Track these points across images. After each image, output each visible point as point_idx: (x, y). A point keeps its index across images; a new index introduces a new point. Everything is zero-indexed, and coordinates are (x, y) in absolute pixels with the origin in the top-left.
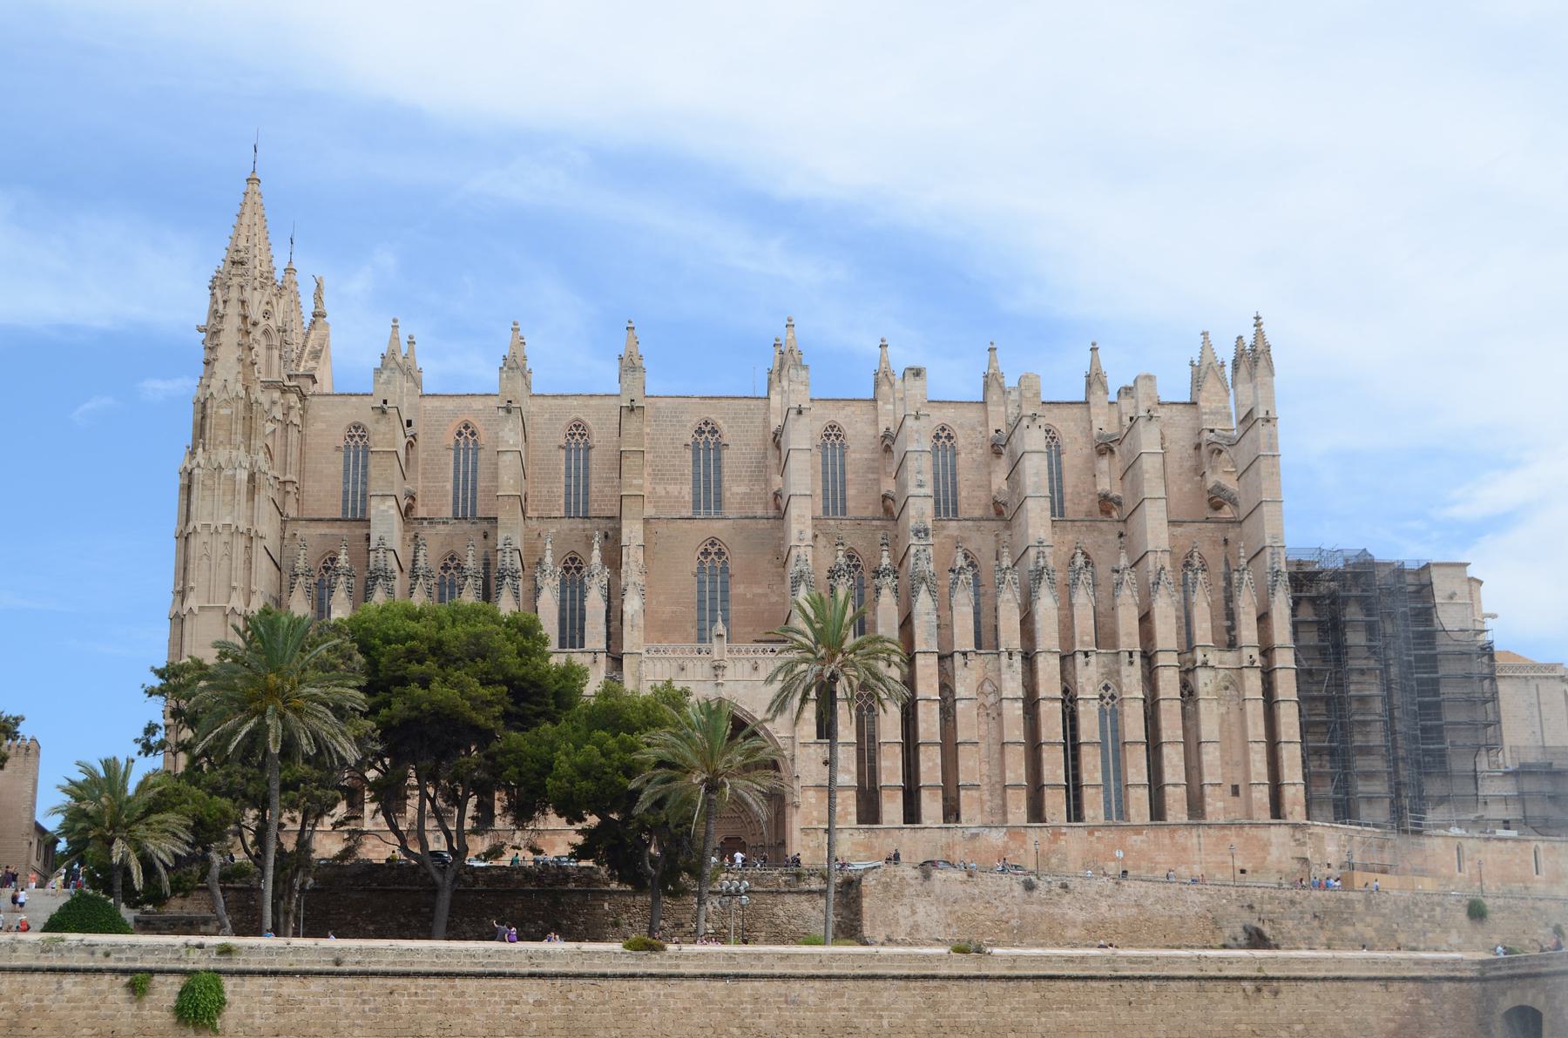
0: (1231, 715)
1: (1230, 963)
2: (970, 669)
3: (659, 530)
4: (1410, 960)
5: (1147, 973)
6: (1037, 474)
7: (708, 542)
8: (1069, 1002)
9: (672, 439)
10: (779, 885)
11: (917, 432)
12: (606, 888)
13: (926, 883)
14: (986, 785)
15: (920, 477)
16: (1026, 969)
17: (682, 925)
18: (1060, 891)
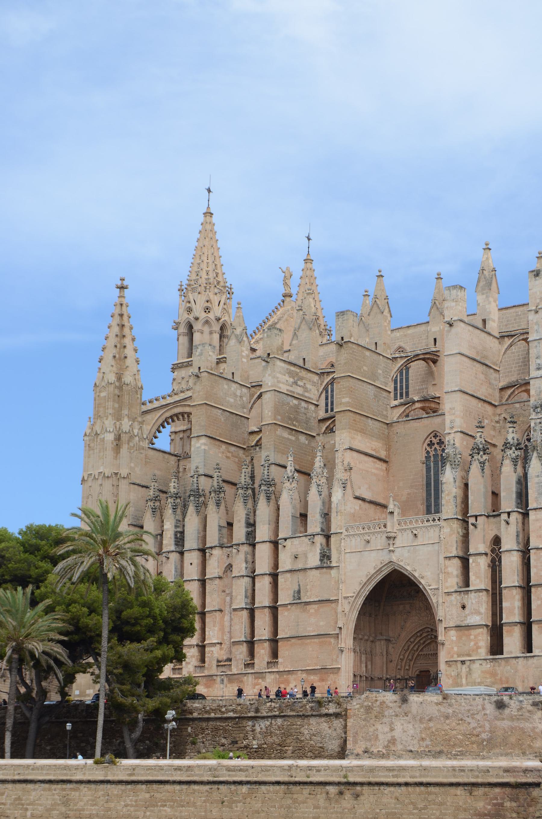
1: (318, 771)
3: (398, 431)
4: (500, 768)
5: (244, 779)
7: (432, 435)
8: (173, 801)
10: (306, 710)
12: (191, 716)
13: (404, 706)
16: (142, 775)
17: (236, 742)
18: (530, 708)
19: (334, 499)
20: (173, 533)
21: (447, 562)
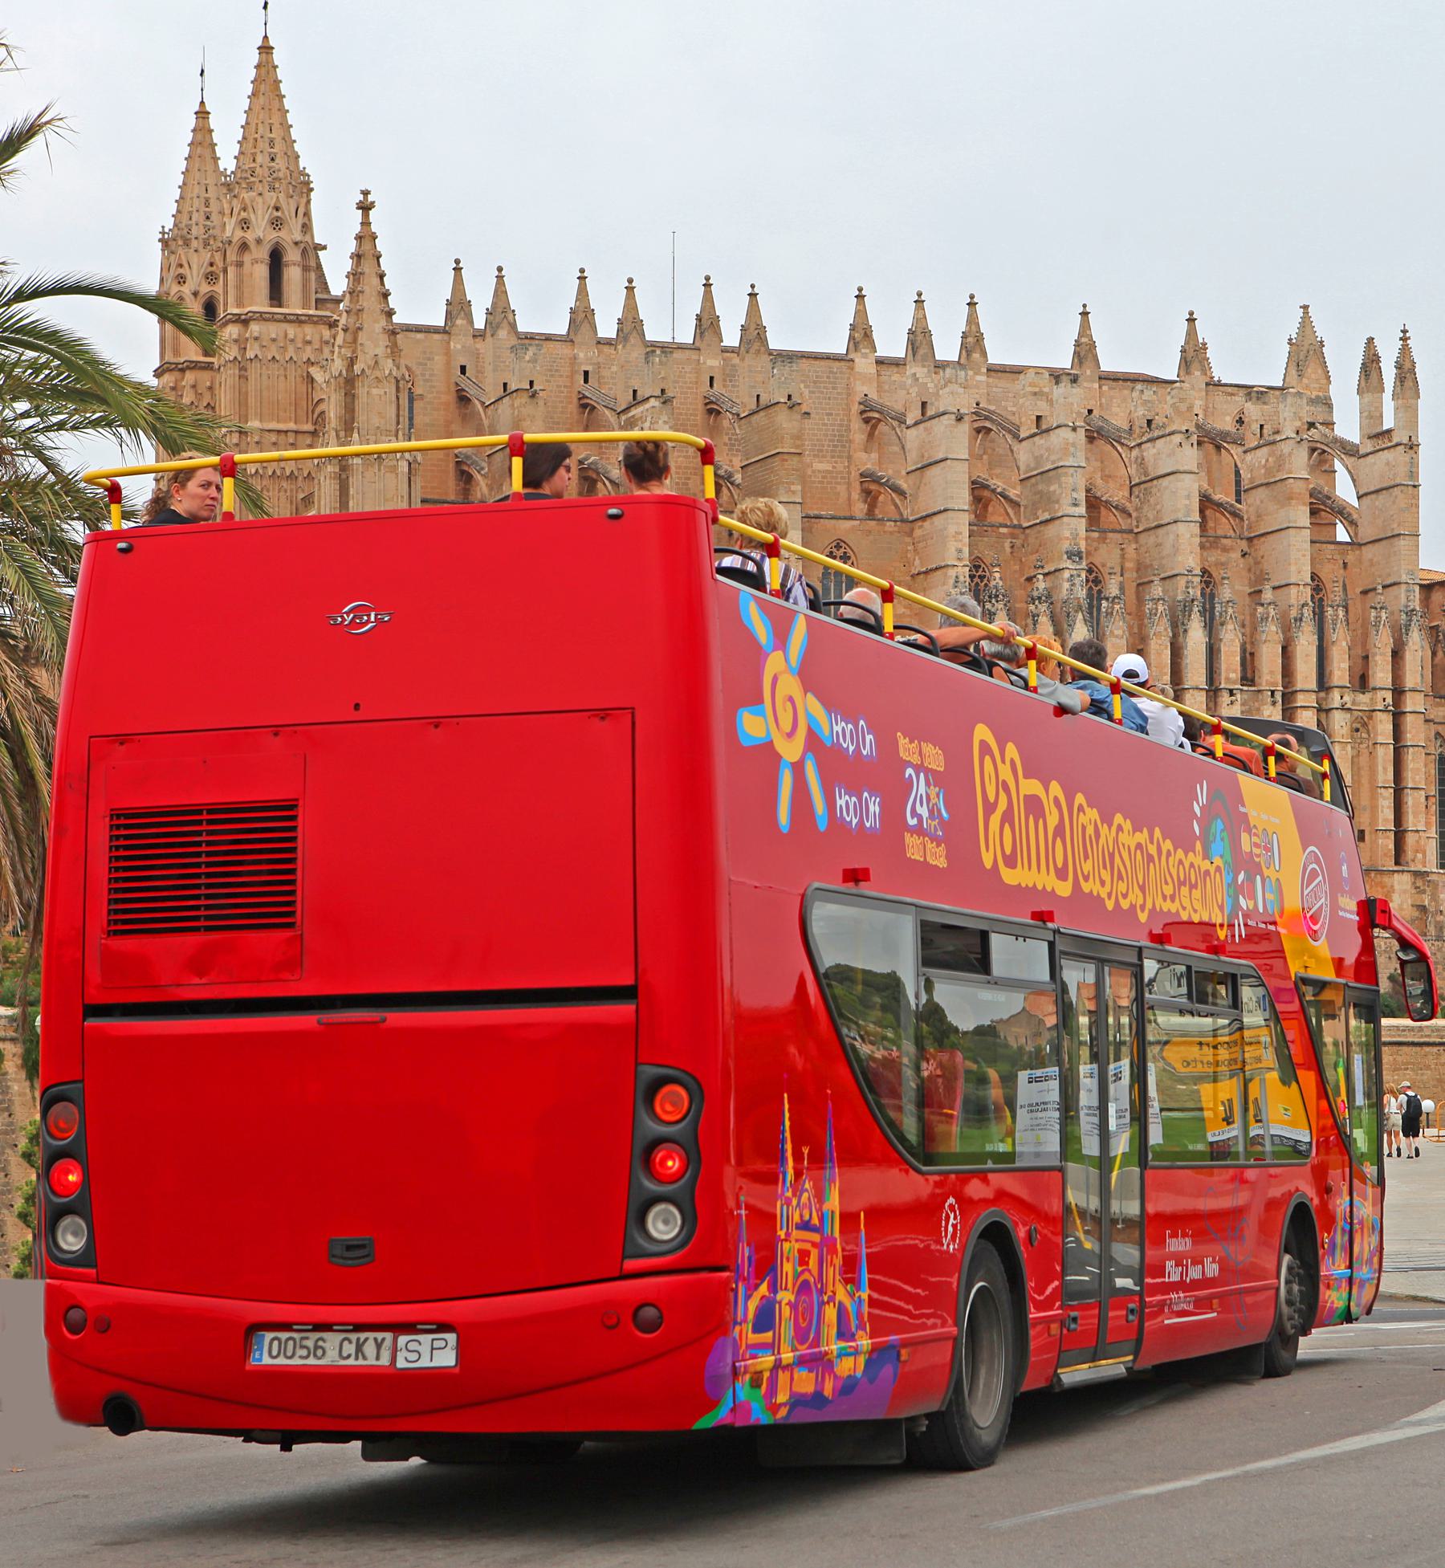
0: (1361, 758)
6: (1188, 497)
11: (1073, 445)
15: (1075, 495)
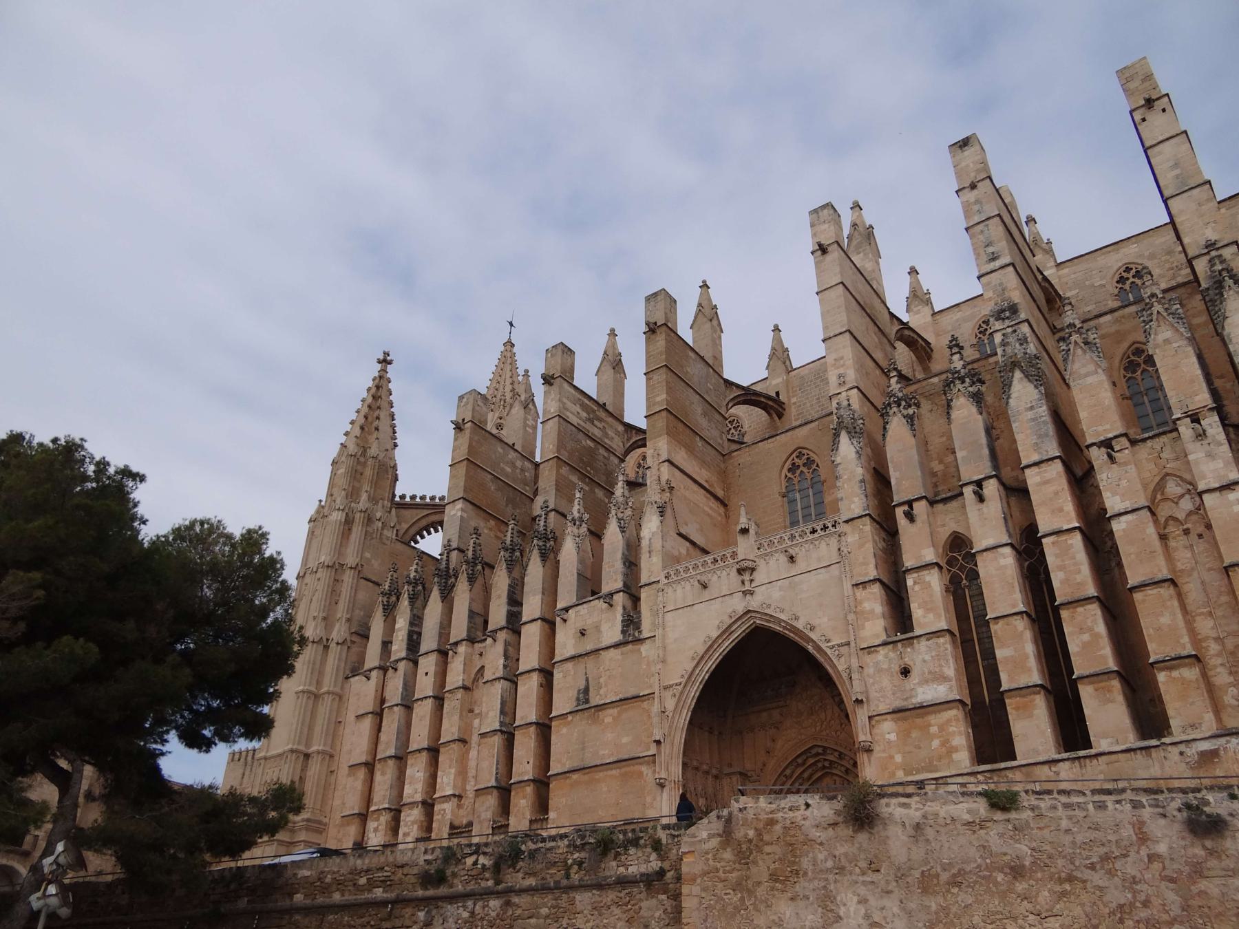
2: (1120, 465)
3: (741, 461)
9: (818, 399)
12: (287, 903)
14: (1219, 655)
15: (990, 249)
19: (646, 533)
20: (407, 632)
21: (860, 593)
